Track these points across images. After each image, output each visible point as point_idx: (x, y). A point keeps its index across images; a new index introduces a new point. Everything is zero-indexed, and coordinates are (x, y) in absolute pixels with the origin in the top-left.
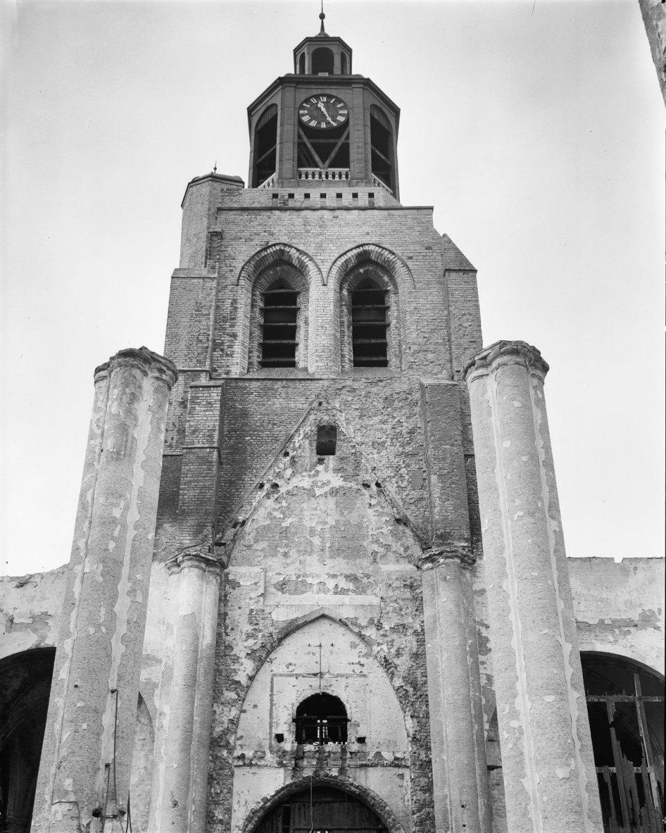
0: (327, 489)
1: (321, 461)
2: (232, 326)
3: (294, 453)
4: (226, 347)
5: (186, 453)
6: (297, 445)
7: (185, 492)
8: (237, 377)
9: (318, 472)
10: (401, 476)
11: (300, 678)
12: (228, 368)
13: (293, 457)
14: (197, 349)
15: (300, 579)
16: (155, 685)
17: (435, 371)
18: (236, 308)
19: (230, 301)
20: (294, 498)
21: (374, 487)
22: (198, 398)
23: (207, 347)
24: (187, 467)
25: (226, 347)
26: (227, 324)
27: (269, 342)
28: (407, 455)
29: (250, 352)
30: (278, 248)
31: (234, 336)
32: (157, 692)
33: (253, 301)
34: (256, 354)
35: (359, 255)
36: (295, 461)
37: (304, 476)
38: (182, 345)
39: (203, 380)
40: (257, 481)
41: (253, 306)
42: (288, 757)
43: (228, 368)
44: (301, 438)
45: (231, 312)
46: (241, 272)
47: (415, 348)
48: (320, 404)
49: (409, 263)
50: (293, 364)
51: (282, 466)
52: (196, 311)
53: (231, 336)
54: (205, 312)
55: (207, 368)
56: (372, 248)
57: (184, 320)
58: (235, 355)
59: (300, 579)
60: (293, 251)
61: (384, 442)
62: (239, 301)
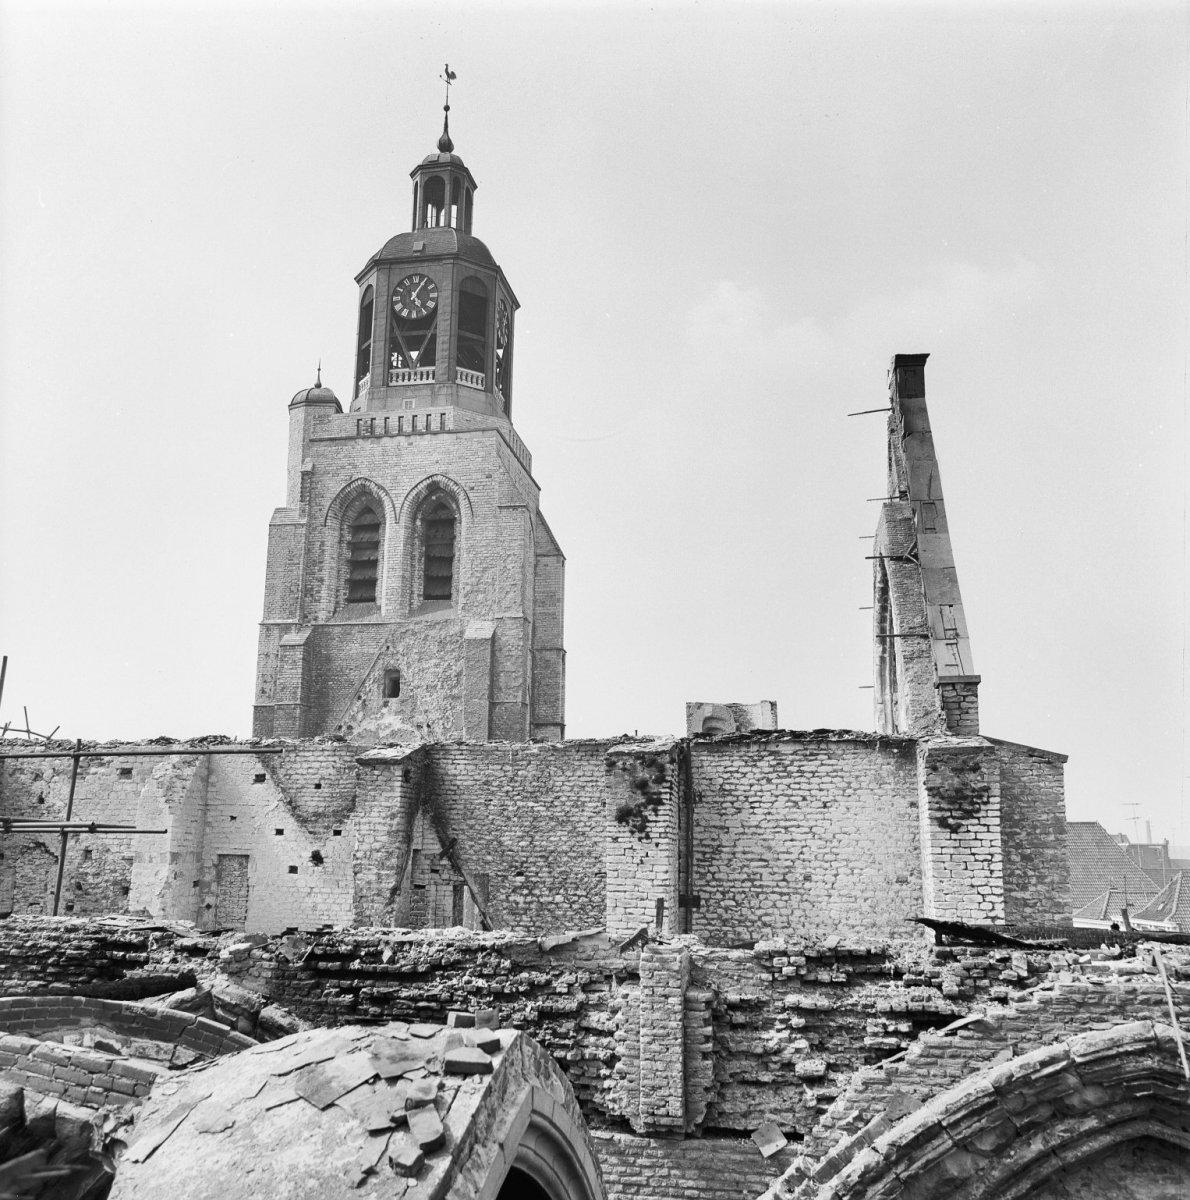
0: (388, 731)
1: (386, 704)
6: (368, 689)
9: (383, 714)
10: (448, 718)
13: (365, 701)
14: (289, 600)
17: (484, 612)
21: (425, 729)
28: (454, 697)
35: (429, 486)
38: (279, 594)
40: (337, 724)
47: (468, 588)
48: (388, 647)
49: (470, 495)
51: (355, 709)
55: (296, 621)
56: (439, 478)
60: (373, 486)
61: (435, 686)
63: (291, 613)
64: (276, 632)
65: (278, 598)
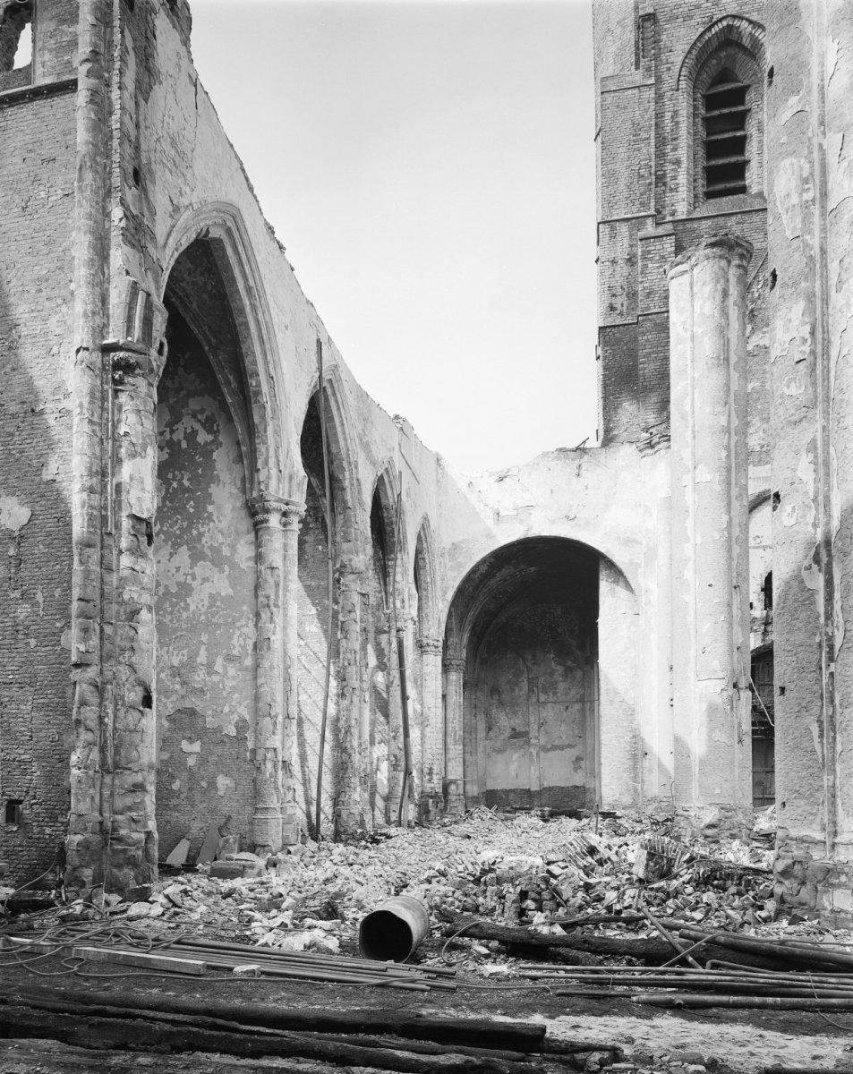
2: (675, 149)
3: (753, 306)
4: (669, 179)
5: (643, 321)
6: (756, 295)
7: (645, 366)
8: (684, 217)
11: (768, 550)
12: (673, 208)
13: (752, 311)
14: (639, 188)
15: (764, 449)
16: (638, 565)
18: (677, 123)
19: (670, 114)
20: (756, 359)
22: (649, 252)
23: (650, 184)
24: (646, 337)
25: (669, 179)
26: (669, 147)
27: (713, 163)
29: (695, 181)
30: (725, 23)
31: (678, 162)
32: (640, 571)
33: (695, 108)
34: (701, 182)
36: (754, 316)
37: (765, 333)
38: (622, 186)
39: (650, 229)
41: (695, 115)
42: (758, 623)
43: (673, 208)
44: (759, 287)
45: (672, 130)
46: (681, 70)
50: (743, 190)
52: (634, 136)
53: (674, 164)
54: (644, 136)
55: (652, 212)
57: (621, 150)
58: (680, 189)
59: (764, 449)
62: (680, 112)
63: (642, 204)
64: (623, 229)
65: (622, 187)
